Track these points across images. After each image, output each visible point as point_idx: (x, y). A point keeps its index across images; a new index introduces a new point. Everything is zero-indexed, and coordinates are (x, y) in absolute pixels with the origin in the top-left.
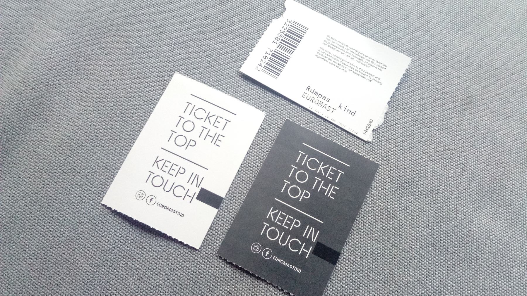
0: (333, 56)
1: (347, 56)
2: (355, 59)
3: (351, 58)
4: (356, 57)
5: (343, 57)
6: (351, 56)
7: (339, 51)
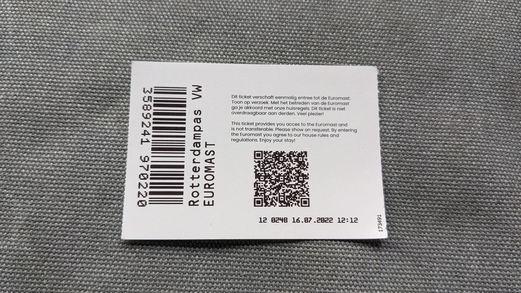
0: (260, 127)
1: (281, 114)
2: (296, 111)
3: (289, 114)
4: (295, 109)
5: (276, 119)
6: (286, 111)
7: (265, 113)
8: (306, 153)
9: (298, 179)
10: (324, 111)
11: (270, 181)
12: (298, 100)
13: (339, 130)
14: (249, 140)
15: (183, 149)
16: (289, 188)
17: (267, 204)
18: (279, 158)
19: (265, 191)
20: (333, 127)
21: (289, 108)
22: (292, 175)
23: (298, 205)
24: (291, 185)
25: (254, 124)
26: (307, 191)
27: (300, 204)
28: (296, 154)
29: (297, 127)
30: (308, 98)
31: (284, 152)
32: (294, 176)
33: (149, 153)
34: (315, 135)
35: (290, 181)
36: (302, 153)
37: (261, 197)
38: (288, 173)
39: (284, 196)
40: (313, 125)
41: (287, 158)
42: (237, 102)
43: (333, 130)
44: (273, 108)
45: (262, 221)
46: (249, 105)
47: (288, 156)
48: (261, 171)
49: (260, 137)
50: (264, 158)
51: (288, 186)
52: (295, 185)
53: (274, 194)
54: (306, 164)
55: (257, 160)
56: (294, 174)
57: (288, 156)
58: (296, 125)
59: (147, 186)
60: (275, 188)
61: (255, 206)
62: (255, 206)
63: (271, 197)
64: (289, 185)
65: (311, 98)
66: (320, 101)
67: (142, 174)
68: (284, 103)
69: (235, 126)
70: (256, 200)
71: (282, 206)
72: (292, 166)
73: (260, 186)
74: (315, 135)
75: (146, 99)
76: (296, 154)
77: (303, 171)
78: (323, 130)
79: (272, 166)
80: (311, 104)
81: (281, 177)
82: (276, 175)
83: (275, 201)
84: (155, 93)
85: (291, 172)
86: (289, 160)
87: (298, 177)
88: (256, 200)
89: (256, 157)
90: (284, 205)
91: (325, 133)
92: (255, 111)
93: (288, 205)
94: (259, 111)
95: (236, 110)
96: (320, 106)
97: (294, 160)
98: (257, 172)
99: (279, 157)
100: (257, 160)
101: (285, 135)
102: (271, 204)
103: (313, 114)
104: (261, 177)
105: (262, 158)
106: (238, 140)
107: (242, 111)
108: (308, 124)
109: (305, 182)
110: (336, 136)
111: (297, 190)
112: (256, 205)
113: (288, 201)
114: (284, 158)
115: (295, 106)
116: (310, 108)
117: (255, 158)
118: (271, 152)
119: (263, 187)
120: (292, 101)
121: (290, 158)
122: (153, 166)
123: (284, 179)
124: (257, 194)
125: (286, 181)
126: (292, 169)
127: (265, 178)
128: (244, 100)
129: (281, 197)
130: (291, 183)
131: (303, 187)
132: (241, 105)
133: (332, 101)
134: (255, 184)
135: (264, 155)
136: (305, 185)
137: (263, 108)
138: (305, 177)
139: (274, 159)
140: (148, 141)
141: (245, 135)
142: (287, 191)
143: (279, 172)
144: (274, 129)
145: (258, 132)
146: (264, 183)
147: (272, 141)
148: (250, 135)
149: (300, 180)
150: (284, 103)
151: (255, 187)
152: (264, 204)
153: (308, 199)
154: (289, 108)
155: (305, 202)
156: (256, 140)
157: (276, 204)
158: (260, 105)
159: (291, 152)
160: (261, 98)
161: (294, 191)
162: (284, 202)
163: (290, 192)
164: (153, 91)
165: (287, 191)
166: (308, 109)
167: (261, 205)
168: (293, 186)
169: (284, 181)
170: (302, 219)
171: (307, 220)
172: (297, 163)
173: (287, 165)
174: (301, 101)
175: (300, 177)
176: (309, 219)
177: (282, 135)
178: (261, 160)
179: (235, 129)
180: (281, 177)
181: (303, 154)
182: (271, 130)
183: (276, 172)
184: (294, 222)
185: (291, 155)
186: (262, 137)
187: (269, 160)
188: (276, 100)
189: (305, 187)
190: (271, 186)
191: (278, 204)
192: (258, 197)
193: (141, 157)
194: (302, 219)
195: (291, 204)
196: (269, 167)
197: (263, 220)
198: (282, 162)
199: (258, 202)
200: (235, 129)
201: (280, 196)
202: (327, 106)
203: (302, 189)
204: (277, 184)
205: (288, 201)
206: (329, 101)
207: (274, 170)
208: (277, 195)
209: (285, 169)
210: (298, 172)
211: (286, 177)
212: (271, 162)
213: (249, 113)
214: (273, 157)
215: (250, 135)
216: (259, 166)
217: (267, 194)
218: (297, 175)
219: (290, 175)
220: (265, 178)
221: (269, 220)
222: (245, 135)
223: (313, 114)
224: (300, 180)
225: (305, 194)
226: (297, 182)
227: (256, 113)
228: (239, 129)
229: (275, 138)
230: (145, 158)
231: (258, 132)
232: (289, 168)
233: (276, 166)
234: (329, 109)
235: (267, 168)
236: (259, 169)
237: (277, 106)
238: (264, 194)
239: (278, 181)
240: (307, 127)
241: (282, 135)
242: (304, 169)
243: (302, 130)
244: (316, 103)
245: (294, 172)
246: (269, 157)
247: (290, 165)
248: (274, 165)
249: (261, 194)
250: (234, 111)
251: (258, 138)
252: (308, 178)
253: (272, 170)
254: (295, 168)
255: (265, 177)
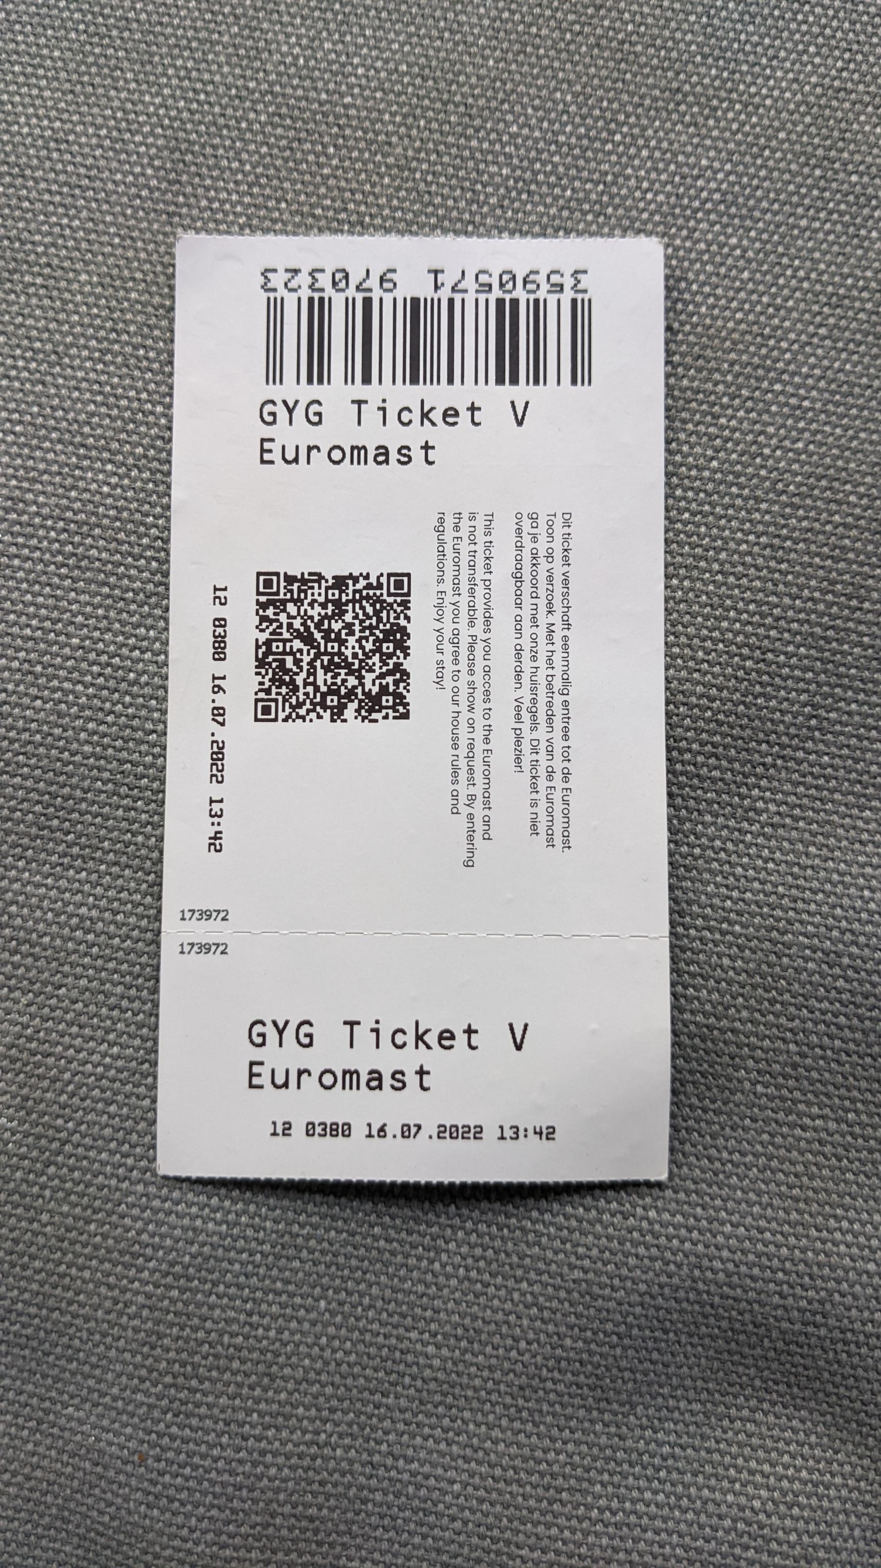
0: (480, 591)
1: (519, 652)
2: (525, 693)
3: (518, 674)
4: (534, 690)
6: (527, 665)
7: (519, 606)
8: (406, 716)
9: (330, 692)
10: (527, 776)
11: (326, 616)
12: (558, 699)
13: (471, 816)
14: (441, 561)
15: (414, 380)
16: (305, 667)
17: (263, 606)
18: (390, 641)
19: (298, 602)
20: (480, 799)
21: (534, 674)
22: (343, 676)
23: (260, 690)
24: (315, 674)
25: (487, 577)
26: (298, 716)
27: (262, 695)
28: (401, 690)
29: (479, 695)
30: (566, 730)
31: (406, 655)
32: (339, 682)
33: (406, 290)
34: (455, 746)
35: (326, 670)
36: (405, 705)
37: (282, 591)
38: (349, 666)
39: (284, 653)
40: (487, 740)
41: (391, 662)
42: (550, 527)
43: (472, 798)
44: (534, 629)
45: (218, 593)
46: (542, 560)
47: (397, 665)
48: (355, 592)
49: (450, 592)
50: (390, 600)
51: (311, 663)
52: (314, 684)
53: (290, 626)
54: (374, 716)
55: (384, 580)
56: (344, 681)
57: (397, 665)
58: (487, 693)
59: (314, 290)
60: (307, 628)
61: (259, 574)
62: (259, 574)
63: (283, 617)
64: (315, 668)
65: (566, 737)
66: (558, 764)
67: (347, 277)
68: (549, 659)
69: (480, 523)
70: (275, 578)
71: (258, 647)
72: (369, 678)
73: (312, 588)
74: (455, 746)
75: (555, 278)
76: (401, 690)
77: (353, 706)
78: (471, 770)
79: (367, 623)
80: (550, 736)
81: (336, 645)
82: (344, 632)
83: (271, 629)
84: (574, 301)
85: (351, 673)
86: (384, 669)
87: (337, 692)
88: (275, 578)
89: (392, 579)
90: (260, 652)
91: (463, 775)
92: (527, 577)
93: (261, 663)
94: (527, 588)
95: (526, 524)
96: (543, 763)
97: (384, 682)
98: (350, 582)
99: (394, 641)
100: (384, 580)
101: (456, 661)
102: (263, 619)
103: (518, 741)
104: (337, 592)
105: (390, 594)
106: (440, 530)
107: (526, 540)
108: (489, 728)
109: (321, 712)
110: (455, 806)
111: (302, 690)
112: (262, 578)
113: (270, 664)
114: (390, 656)
115: (542, 690)
116: (535, 735)
117: (390, 575)
118: (408, 618)
119: (310, 598)
120: (558, 684)
121: (390, 673)
122: (367, 302)
123: (332, 655)
124: (290, 579)
125: (326, 659)
126: (360, 678)
127: (334, 602)
128: (558, 546)
129: (281, 644)
130: (320, 672)
131: (308, 706)
132: (543, 538)
133: (557, 796)
134: (319, 574)
135: (399, 599)
136: (314, 710)
137: (535, 601)
138: (338, 714)
139: (388, 626)
140: (436, 288)
141: (457, 551)
142: (297, 662)
143: (352, 641)
144: (472, 631)
145: (464, 587)
146: (322, 599)
147: (438, 626)
148: (457, 564)
149: (329, 698)
150: (549, 659)
151: (310, 574)
152: (263, 599)
153: (275, 720)
154: (534, 674)
155: (266, 710)
156: (440, 581)
157: (262, 631)
158: (542, 593)
159: (408, 675)
160: (565, 595)
161: (299, 680)
162: (269, 652)
163: (295, 669)
164: (579, 297)
165: (297, 662)
166: (534, 728)
167: (261, 589)
168: (311, 679)
169: (326, 653)
170: (221, 700)
171: (218, 713)
172: (375, 690)
173: (370, 662)
174: (558, 709)
175: (335, 698)
176: (220, 719)
177: (456, 654)
178: (385, 591)
179: (472, 523)
180: (336, 645)
181: (401, 709)
182: (471, 623)
183: (351, 633)
184: (214, 678)
185: (398, 676)
186: (449, 598)
187: (384, 614)
188: (557, 638)
189: (308, 711)
190: (311, 618)
191: (263, 637)
192: (282, 584)
193: (394, 271)
194: (221, 700)
195: (263, 671)
196: (365, 614)
197: (219, 596)
198: (379, 650)
199: (268, 584)
200: (472, 523)
201: (285, 641)
202: (542, 783)
203: (304, 703)
204: (318, 636)
205: (270, 664)
206: (559, 789)
207: (357, 628)
208: (286, 635)
209: (360, 656)
210: (351, 692)
211: (336, 659)
212: (380, 620)
213: (519, 562)
214: (392, 625)
215: (457, 564)
216: (369, 586)
217: (291, 608)
218: (343, 691)
219: (343, 672)
220: (334, 602)
221: (220, 612)
222: (457, 551)
223: (518, 741)
224: (329, 698)
225: (288, 710)
226: (324, 689)
227: (519, 579)
228: (472, 533)
229: (448, 634)
230: (391, 280)
231: (464, 587)
232: (361, 667)
233: (367, 633)
234: (535, 789)
235: (362, 608)
236: (359, 586)
237: (542, 640)
238: (292, 600)
239: (327, 639)
240: (479, 724)
241: (456, 654)
242: (358, 711)
243: (471, 709)
244: (550, 753)
245: (352, 681)
246: (392, 615)
247: (370, 670)
248: (371, 627)
249: (291, 591)
250: (525, 518)
251: (448, 586)
252: (333, 720)
253: (357, 622)
254: (362, 685)
255: (338, 603)
